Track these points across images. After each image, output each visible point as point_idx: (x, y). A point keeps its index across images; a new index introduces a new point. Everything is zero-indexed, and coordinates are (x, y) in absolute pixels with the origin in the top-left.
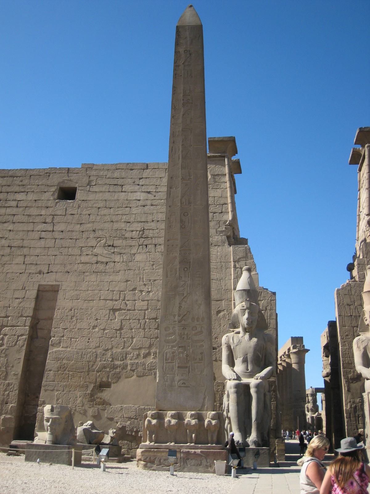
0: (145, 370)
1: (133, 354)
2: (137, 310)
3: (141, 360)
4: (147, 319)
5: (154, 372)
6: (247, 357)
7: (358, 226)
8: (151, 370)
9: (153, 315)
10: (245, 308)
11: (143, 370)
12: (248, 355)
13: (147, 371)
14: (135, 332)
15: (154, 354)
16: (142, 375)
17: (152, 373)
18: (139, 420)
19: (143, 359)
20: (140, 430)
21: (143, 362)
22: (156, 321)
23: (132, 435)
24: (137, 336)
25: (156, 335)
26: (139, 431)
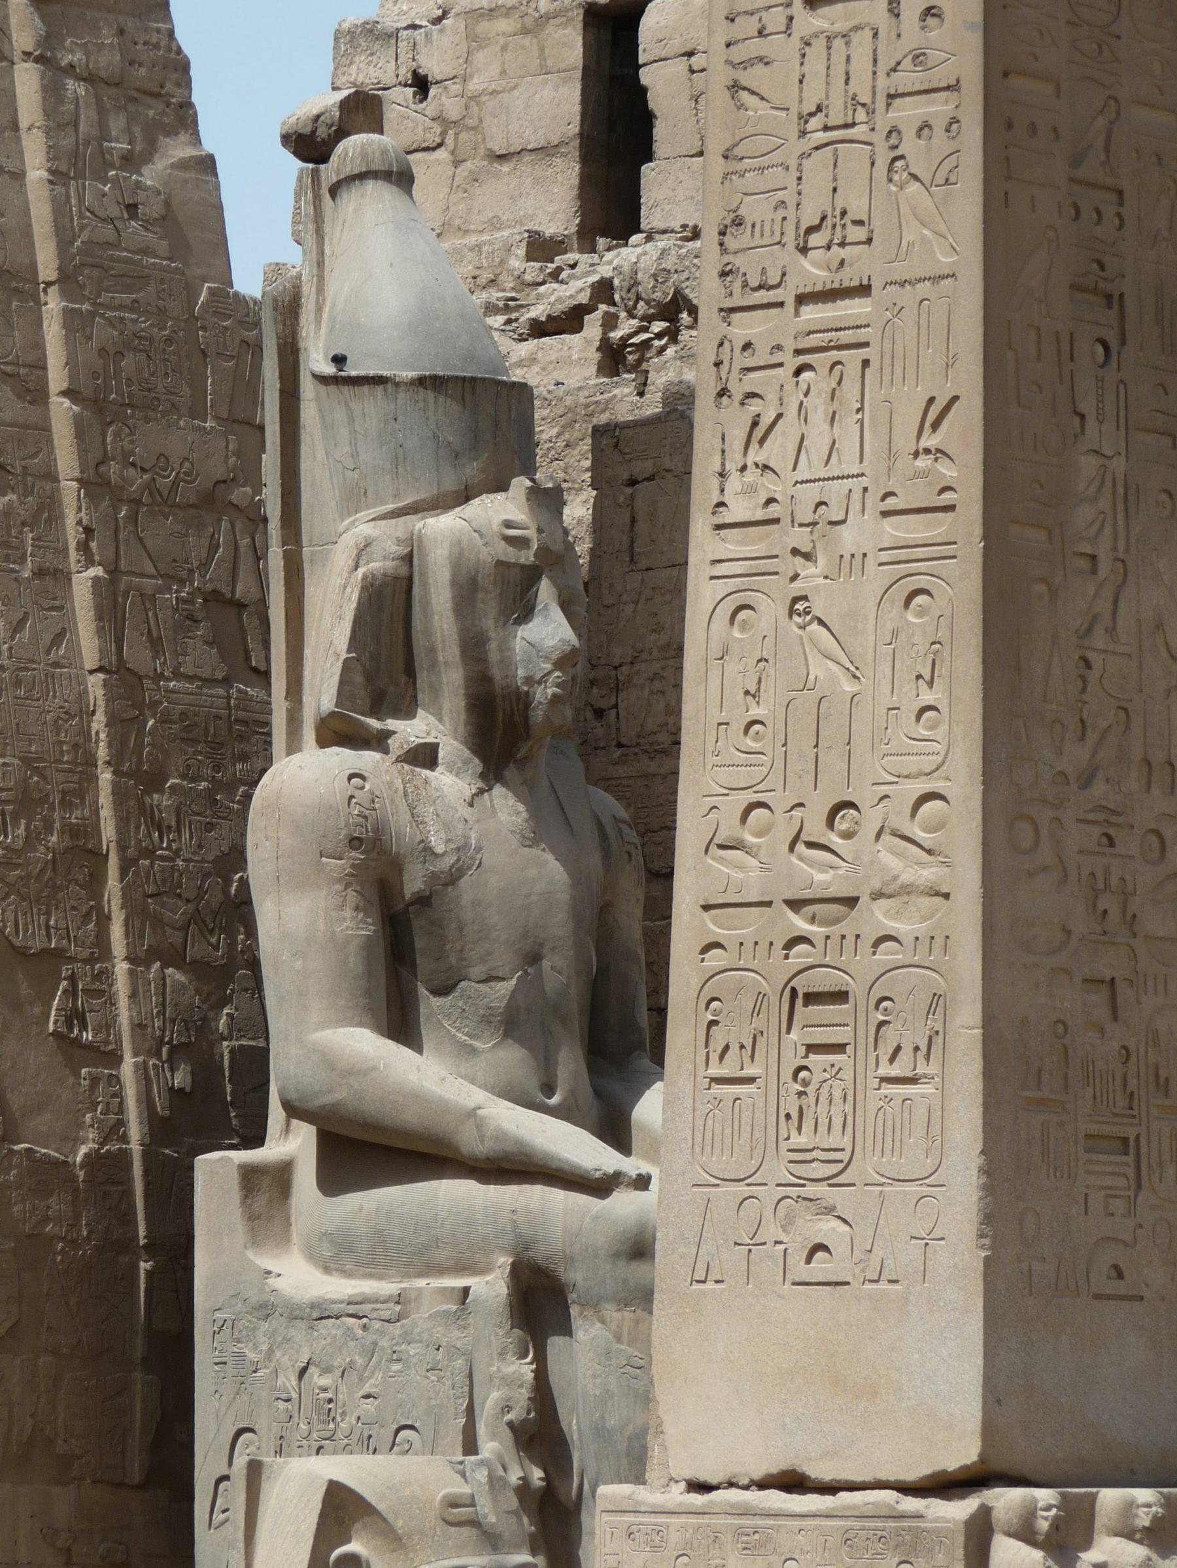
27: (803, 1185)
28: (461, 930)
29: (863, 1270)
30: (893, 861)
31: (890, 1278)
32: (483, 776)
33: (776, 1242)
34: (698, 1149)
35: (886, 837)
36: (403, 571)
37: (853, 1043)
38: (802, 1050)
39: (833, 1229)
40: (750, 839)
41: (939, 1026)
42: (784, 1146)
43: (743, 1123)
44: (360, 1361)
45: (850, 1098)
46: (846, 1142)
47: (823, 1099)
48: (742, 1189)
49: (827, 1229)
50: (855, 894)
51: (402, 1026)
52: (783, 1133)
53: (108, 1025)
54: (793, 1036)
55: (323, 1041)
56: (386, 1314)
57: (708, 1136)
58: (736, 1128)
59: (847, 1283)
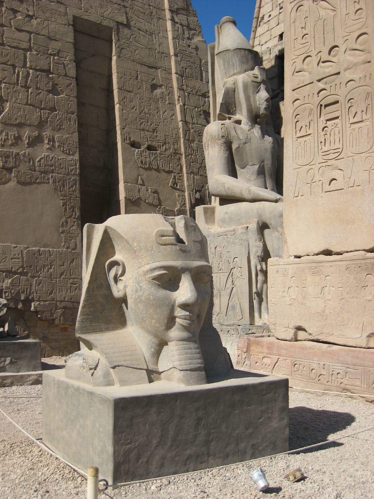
0: (35, 171)
1: (7, 135)
2: (9, 46)
3: (23, 150)
4: (31, 69)
5: (52, 177)
6: (263, 166)
7: (255, 32)
8: (46, 172)
9: (43, 63)
10: (259, 80)
11: (30, 171)
12: (265, 163)
13: (37, 173)
14: (8, 89)
15: (49, 140)
16: (28, 180)
17: (48, 179)
18: (31, 277)
19: (28, 147)
20: (33, 298)
21: (29, 154)
22: (48, 76)
23: (16, 308)
24: (12, 98)
25: (51, 105)
26: (33, 300)
27: (327, 162)
28: (246, 155)
29: (348, 184)
30: (351, 58)
31: (357, 185)
32: (251, 126)
33: (319, 181)
34: (294, 159)
35: (348, 52)
36: (233, 87)
37: (341, 115)
38: (325, 122)
39: (338, 173)
40: (305, 67)
41: (370, 103)
42: (320, 151)
43: (307, 148)
44: (226, 244)
45: (341, 132)
46: (341, 146)
47: (332, 135)
48: (308, 167)
49: (336, 174)
50: (339, 71)
51: (233, 173)
52: (320, 148)
53: (183, 185)
54: (322, 118)
55: (218, 179)
56: (231, 234)
57: (297, 154)
58: (305, 150)
59: (343, 189)
